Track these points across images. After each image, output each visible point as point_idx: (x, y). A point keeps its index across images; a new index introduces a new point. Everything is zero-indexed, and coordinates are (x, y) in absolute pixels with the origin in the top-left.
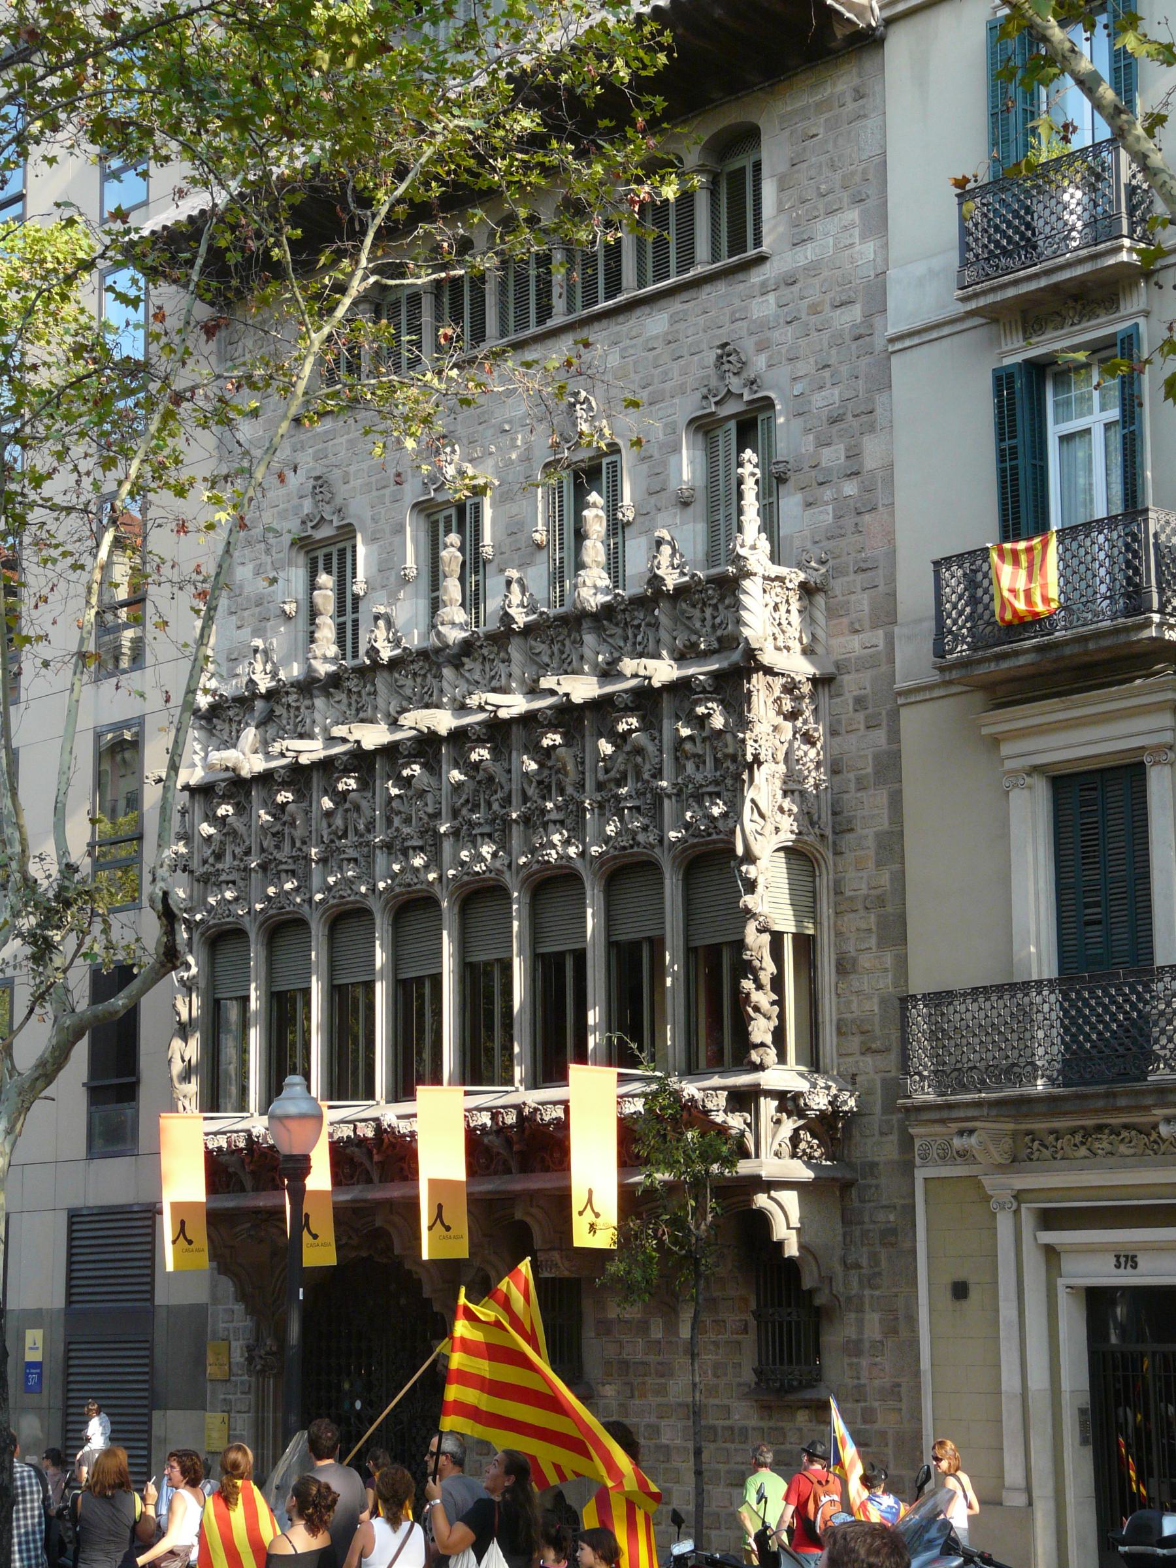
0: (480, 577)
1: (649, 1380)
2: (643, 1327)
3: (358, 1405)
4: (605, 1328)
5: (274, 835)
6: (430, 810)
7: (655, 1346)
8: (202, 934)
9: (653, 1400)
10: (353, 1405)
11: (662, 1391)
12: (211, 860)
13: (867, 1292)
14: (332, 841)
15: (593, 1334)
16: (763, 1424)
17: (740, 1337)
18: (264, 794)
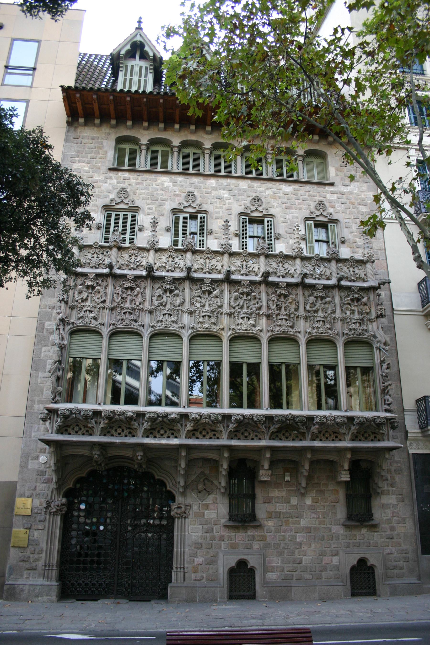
0: (205, 238)
1: (291, 520)
2: (287, 501)
3: (102, 528)
4: (268, 501)
5: (122, 298)
6: (219, 304)
7: (295, 507)
8: (71, 328)
9: (293, 527)
10: (98, 528)
11: (298, 523)
12: (80, 301)
13: (390, 489)
14: (159, 306)
15: (261, 502)
16: (345, 533)
17: (335, 504)
18: (114, 282)
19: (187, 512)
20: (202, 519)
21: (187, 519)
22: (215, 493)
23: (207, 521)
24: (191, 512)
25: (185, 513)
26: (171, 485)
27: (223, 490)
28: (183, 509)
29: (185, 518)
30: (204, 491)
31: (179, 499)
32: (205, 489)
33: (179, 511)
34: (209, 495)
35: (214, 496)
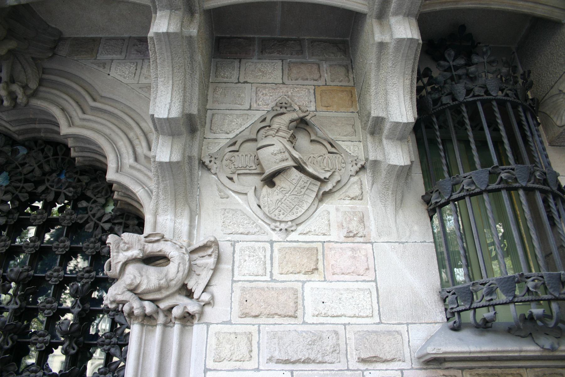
19: (196, 285)
20: (288, 325)
21: (197, 329)
22: (355, 191)
23: (316, 339)
24: (220, 288)
25: (189, 294)
26: (129, 160)
27: (399, 155)
28: (173, 271)
29: (187, 318)
30: (295, 174)
31: (164, 221)
32: (300, 168)
33: (151, 277)
34: (323, 196)
35: (347, 205)
